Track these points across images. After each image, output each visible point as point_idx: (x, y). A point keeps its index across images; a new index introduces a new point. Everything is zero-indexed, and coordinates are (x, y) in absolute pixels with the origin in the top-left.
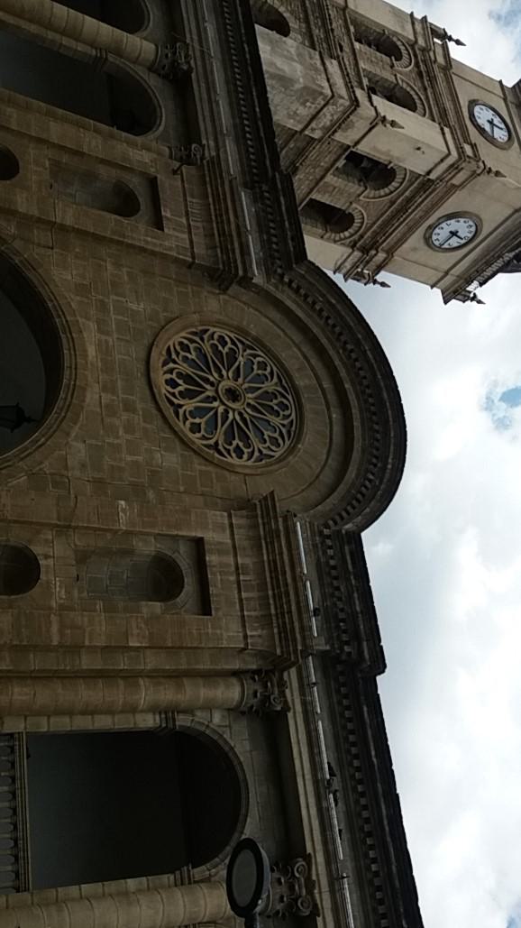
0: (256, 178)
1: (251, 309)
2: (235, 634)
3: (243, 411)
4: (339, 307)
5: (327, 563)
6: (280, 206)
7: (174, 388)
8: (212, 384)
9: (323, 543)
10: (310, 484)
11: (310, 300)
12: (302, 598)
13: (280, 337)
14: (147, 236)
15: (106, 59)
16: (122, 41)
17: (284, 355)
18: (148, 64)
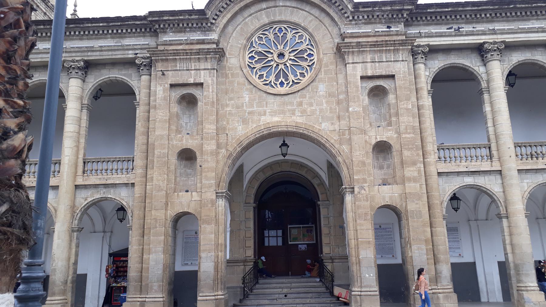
0: (148, 30)
1: (230, 41)
3: (289, 51)
5: (366, 19)
6: (169, 20)
7: (284, 84)
8: (278, 65)
9: (355, 20)
10: (321, 21)
11: (222, 10)
12: (384, 34)
13: (242, 28)
14: (209, 91)
15: (88, 104)
16: (76, 97)
17: (252, 27)
18: (82, 82)
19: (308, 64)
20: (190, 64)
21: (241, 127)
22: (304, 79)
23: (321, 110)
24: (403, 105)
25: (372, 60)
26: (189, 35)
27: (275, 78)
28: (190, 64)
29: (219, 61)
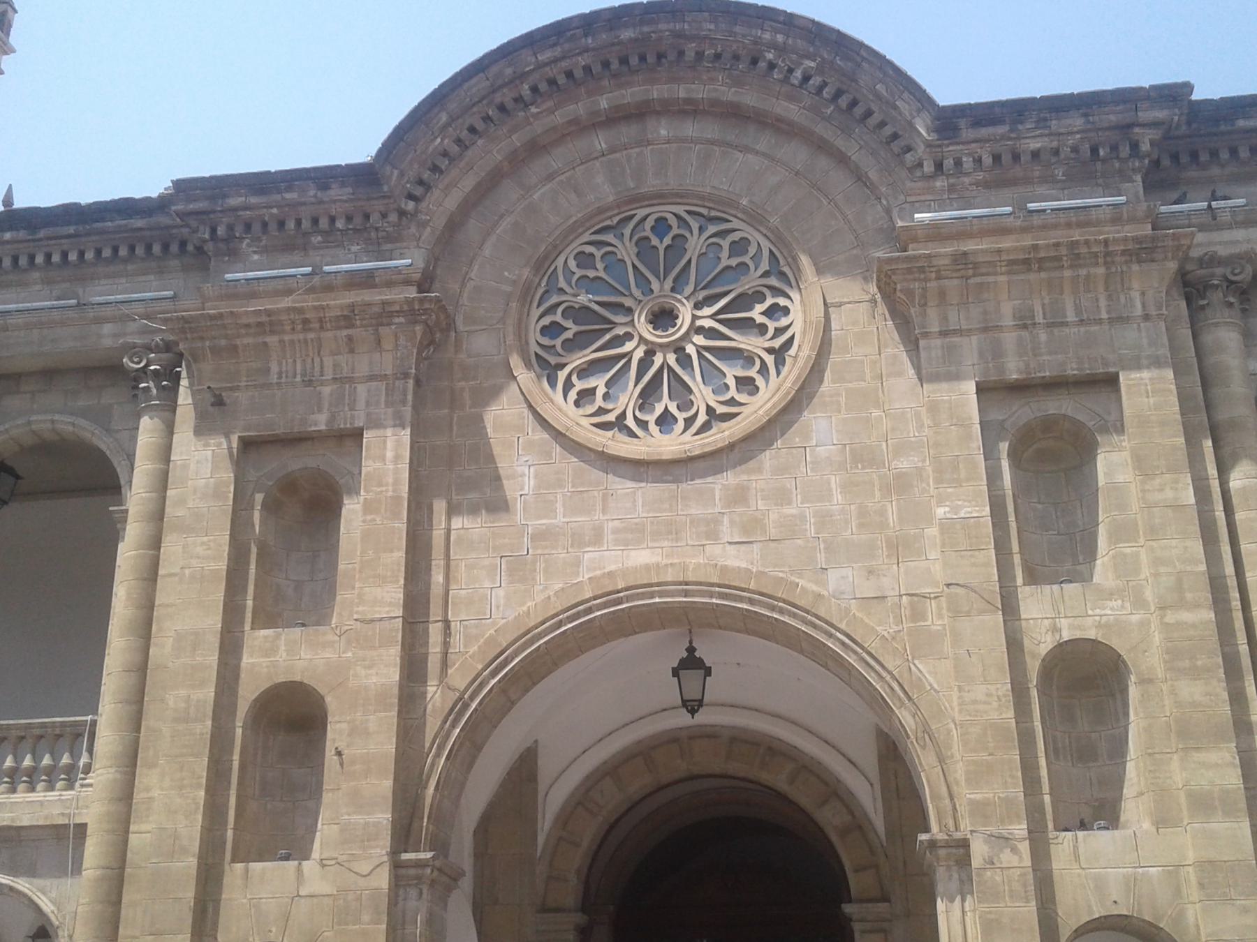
1: (472, 275)
2: (1144, 334)
4: (453, 106)
7: (676, 420)
8: (650, 353)
11: (444, 163)
12: (1062, 218)
14: (383, 458)
19: (767, 345)
20: (317, 360)
21: (501, 592)
22: (753, 399)
23: (824, 519)
24: (1161, 490)
25: (1021, 318)
26: (318, 258)
27: (641, 401)
28: (317, 360)
29: (429, 345)
